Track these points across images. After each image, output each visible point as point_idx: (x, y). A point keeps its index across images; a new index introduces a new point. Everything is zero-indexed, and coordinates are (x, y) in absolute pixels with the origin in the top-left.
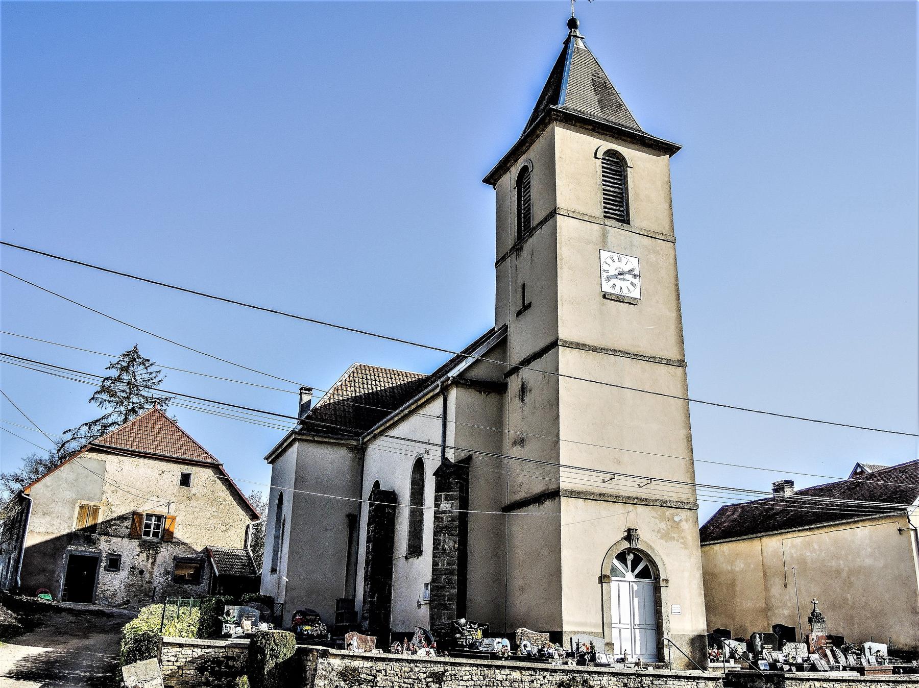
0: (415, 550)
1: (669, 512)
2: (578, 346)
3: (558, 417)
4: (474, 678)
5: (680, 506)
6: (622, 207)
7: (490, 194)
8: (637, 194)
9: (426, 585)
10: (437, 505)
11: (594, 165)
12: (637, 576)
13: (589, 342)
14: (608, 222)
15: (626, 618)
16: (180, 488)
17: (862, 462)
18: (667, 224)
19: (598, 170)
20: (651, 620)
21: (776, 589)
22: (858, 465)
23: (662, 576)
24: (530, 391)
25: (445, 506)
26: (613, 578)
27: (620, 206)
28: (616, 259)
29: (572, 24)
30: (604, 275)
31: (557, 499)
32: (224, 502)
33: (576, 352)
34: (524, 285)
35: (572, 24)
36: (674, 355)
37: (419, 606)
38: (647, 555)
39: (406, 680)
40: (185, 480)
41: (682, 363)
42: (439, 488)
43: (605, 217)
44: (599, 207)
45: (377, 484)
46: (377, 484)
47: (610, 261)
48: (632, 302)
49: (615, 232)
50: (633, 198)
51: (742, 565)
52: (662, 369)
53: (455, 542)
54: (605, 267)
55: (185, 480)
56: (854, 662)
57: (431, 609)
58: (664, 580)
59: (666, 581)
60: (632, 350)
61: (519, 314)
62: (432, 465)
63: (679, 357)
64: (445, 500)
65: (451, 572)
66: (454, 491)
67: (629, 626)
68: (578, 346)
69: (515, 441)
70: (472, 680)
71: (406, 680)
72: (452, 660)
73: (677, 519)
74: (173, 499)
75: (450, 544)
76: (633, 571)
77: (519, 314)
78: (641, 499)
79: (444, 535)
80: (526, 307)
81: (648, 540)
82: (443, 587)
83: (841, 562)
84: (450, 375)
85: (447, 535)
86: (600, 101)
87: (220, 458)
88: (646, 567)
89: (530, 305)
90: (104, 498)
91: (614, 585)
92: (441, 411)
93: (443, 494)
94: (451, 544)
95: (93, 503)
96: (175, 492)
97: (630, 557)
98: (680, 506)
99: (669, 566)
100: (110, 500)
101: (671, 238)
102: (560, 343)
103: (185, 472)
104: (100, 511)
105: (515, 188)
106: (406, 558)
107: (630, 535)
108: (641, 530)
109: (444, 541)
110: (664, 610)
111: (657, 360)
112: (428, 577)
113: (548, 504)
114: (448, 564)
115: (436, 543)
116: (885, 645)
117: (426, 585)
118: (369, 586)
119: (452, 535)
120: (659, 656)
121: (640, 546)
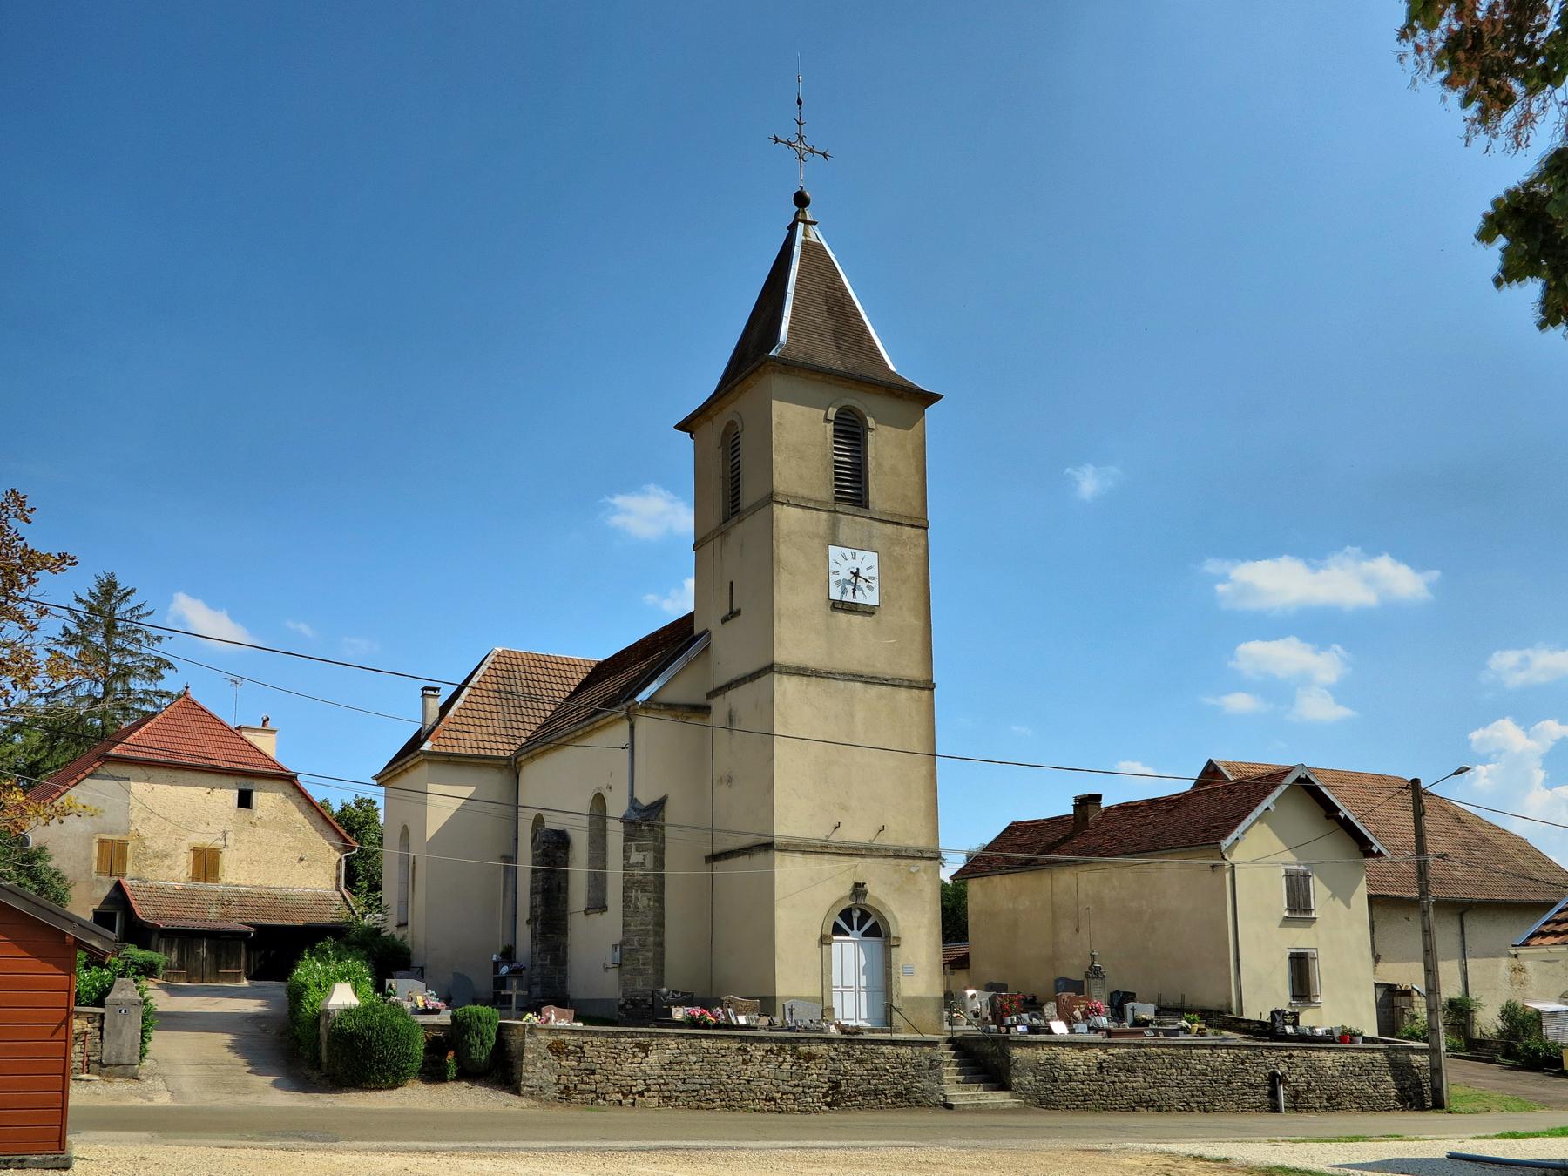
0: (598, 905)
1: (903, 862)
2: (801, 672)
3: (772, 758)
4: (680, 1047)
5: (918, 855)
6: (860, 482)
7: (685, 441)
8: (879, 465)
9: (615, 947)
10: (626, 857)
11: (823, 429)
12: (863, 935)
13: (812, 664)
14: (840, 508)
15: (850, 981)
16: (237, 810)
17: (1216, 759)
18: (916, 503)
19: (828, 436)
20: (880, 983)
21: (1066, 935)
22: (1210, 762)
23: (894, 934)
24: (740, 721)
25: (635, 857)
26: (835, 938)
27: (857, 482)
28: (849, 556)
29: (801, 200)
30: (833, 578)
31: (771, 852)
32: (303, 829)
33: (795, 679)
34: (732, 583)
35: (801, 200)
36: (914, 672)
37: (606, 969)
38: (876, 910)
39: (613, 1050)
40: (245, 800)
41: (929, 686)
42: (628, 838)
43: (836, 498)
44: (829, 487)
45: (539, 821)
46: (539, 821)
47: (840, 560)
48: (867, 611)
49: (849, 524)
50: (874, 472)
51: (1027, 903)
52: (903, 694)
53: (649, 899)
54: (833, 567)
55: (245, 800)
56: (1293, 1031)
57: (621, 974)
58: (894, 938)
59: (898, 939)
60: (866, 671)
61: (725, 620)
62: (617, 807)
63: (925, 677)
64: (637, 851)
65: (646, 934)
66: (647, 841)
67: (853, 989)
68: (801, 672)
69: (721, 779)
70: (678, 1048)
71: (613, 1050)
72: (658, 1030)
73: (913, 870)
74: (230, 827)
75: (643, 900)
76: (859, 929)
77: (725, 620)
78: (871, 849)
79: (637, 891)
80: (734, 614)
81: (880, 893)
82: (636, 950)
83: (1144, 903)
84: (638, 699)
85: (639, 891)
86: (835, 330)
87: (290, 766)
88: (875, 925)
89: (738, 612)
90: (133, 829)
91: (835, 947)
92: (627, 740)
93: (633, 843)
94: (645, 902)
95: (116, 837)
96: (232, 816)
97: (856, 914)
98: (918, 855)
99: (902, 924)
100: (141, 831)
101: (921, 523)
102: (775, 669)
103: (242, 788)
104: (129, 847)
105: (719, 447)
106: (586, 912)
107: (858, 890)
108: (870, 884)
109: (637, 898)
110: (893, 971)
111: (897, 682)
112: (617, 936)
113: (760, 858)
114: (641, 924)
115: (626, 900)
116: (1153, 1006)
117: (615, 947)
118: (539, 946)
119: (646, 891)
120: (888, 1021)
121: (868, 901)
